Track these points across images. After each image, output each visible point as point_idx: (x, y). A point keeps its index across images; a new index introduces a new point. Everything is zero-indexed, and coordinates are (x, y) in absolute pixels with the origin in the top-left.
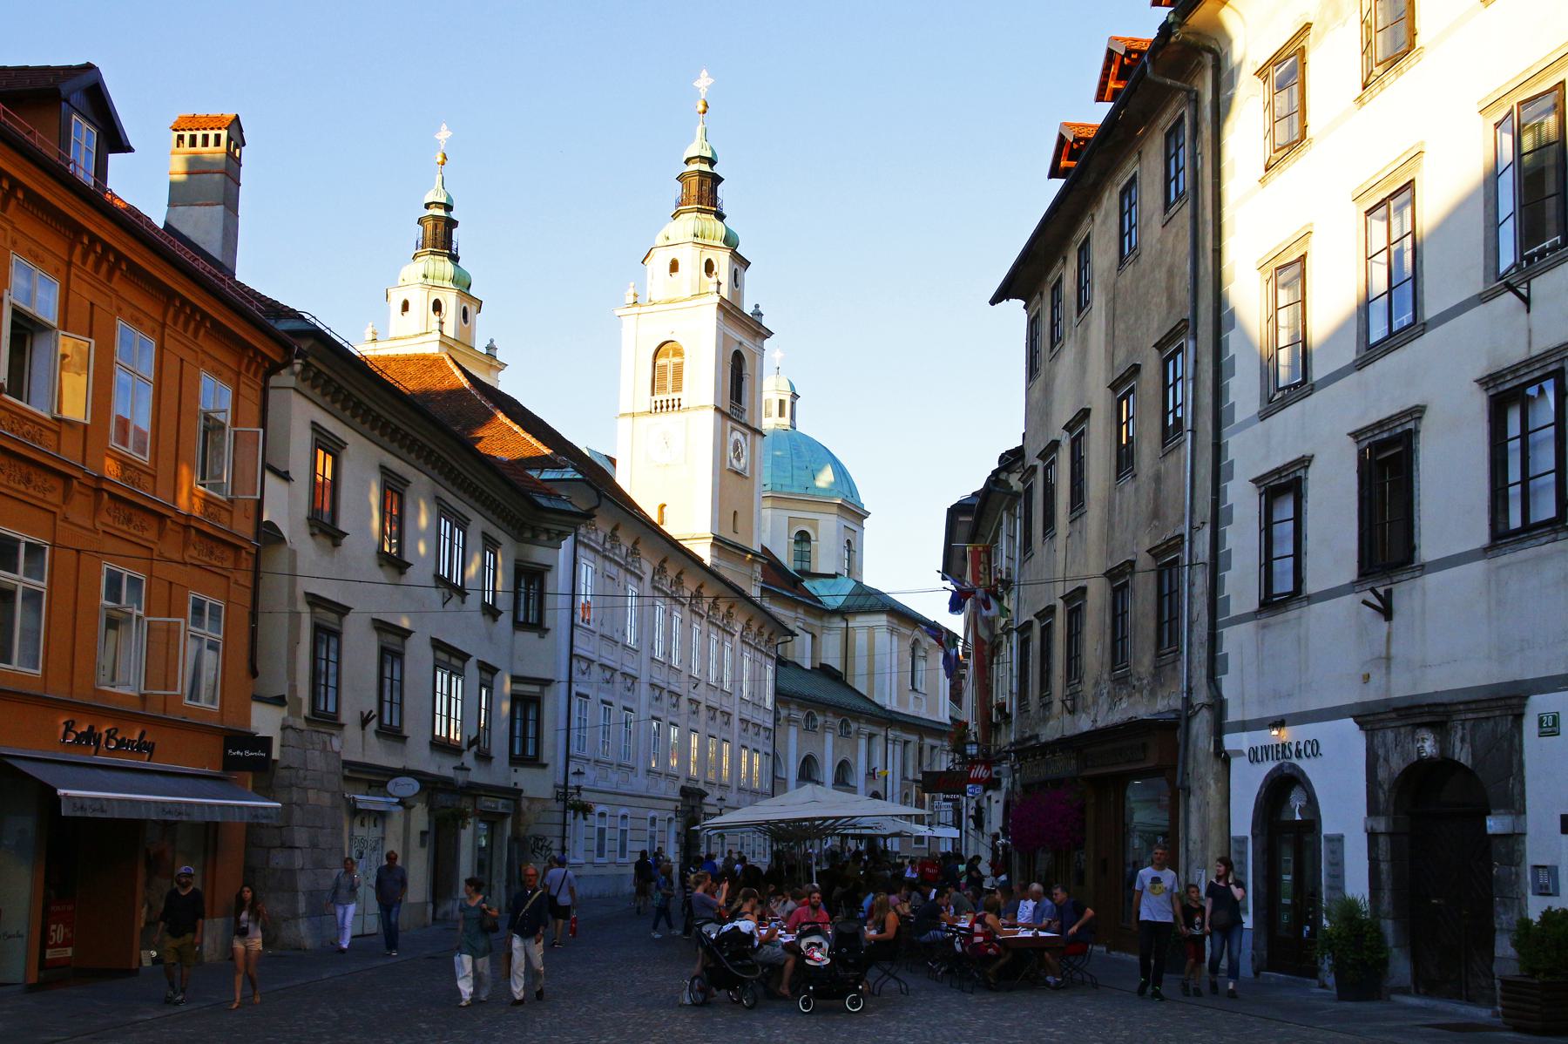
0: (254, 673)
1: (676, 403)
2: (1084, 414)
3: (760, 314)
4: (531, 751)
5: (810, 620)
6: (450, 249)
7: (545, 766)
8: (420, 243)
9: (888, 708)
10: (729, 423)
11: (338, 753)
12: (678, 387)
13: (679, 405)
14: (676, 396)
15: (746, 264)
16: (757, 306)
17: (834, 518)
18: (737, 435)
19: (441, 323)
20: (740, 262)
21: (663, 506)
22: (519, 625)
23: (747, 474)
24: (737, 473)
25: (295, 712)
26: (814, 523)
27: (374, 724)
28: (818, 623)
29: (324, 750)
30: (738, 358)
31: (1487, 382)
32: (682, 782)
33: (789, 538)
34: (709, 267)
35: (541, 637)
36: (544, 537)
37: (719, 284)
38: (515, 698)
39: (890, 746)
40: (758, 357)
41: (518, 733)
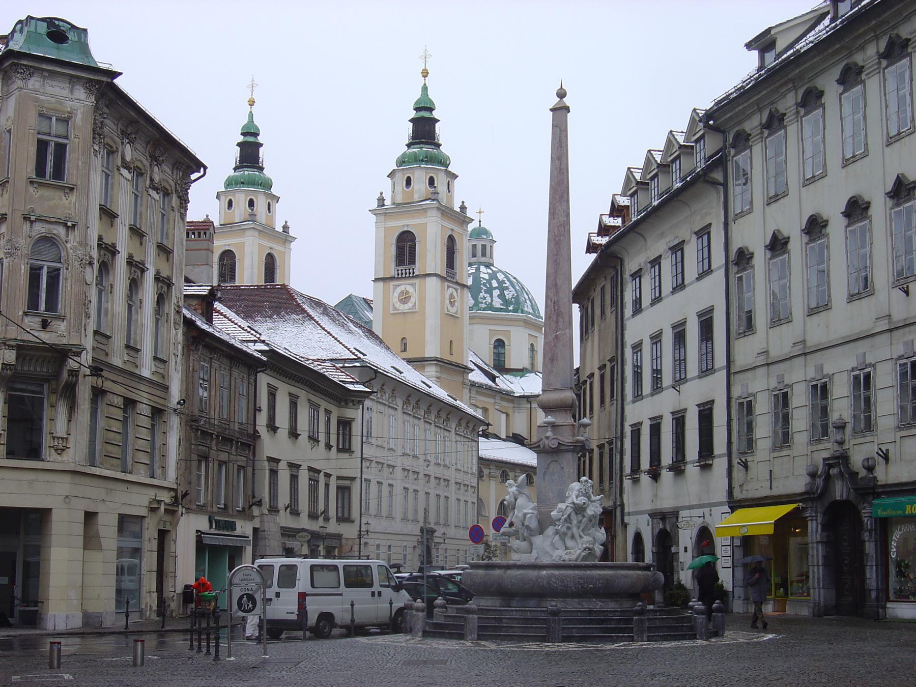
1: (411, 271)
2: (592, 375)
4: (346, 515)
5: (505, 404)
7: (353, 522)
8: (238, 159)
10: (446, 284)
11: (279, 523)
12: (413, 261)
13: (414, 273)
15: (455, 176)
16: (463, 202)
17: (521, 329)
22: (339, 450)
27: (288, 510)
28: (511, 405)
29: (275, 523)
30: (451, 239)
31: (673, 413)
32: (421, 524)
33: (490, 344)
34: (431, 181)
36: (351, 404)
38: (338, 488)
41: (340, 505)
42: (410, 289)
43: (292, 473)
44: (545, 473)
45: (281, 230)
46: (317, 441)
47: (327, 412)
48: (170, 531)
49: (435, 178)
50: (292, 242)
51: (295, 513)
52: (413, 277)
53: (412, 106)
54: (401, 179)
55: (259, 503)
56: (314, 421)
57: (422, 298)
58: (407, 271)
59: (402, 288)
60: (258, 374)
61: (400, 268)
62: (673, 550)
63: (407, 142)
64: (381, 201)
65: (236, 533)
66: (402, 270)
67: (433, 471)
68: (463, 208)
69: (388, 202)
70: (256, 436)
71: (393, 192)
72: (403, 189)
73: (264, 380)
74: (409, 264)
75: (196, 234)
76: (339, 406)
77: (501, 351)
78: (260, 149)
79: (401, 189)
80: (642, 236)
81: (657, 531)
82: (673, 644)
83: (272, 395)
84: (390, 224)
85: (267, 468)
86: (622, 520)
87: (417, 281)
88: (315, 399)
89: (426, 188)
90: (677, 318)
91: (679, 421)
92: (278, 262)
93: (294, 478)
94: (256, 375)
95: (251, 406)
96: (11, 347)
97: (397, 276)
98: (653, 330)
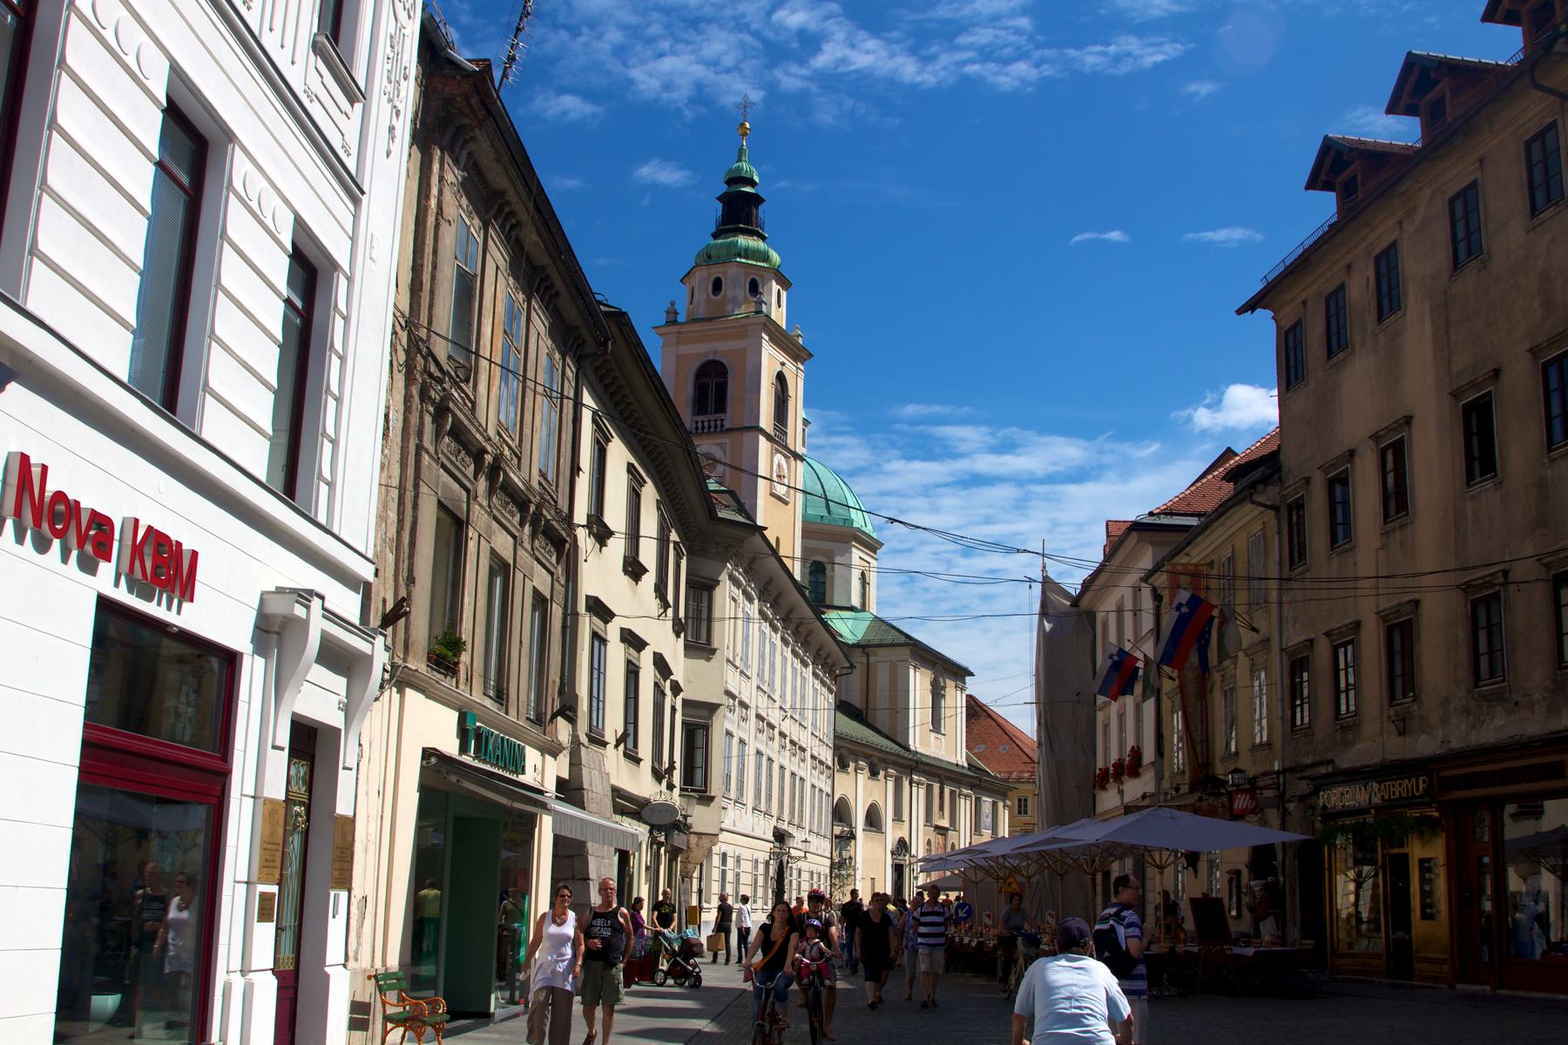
1: (719, 423)
9: (912, 748)
12: (721, 406)
13: (722, 426)
14: (722, 416)
18: (778, 458)
24: (779, 498)
26: (830, 555)
27: (622, 747)
30: (781, 378)
35: (709, 660)
39: (914, 789)
43: (630, 658)
52: (722, 431)
53: (723, 178)
54: (703, 277)
58: (712, 423)
61: (700, 418)
63: (713, 230)
64: (671, 312)
65: (522, 778)
66: (703, 422)
69: (681, 318)
71: (691, 303)
72: (708, 295)
74: (716, 412)
77: (820, 578)
87: (726, 440)
93: (632, 672)
97: (694, 431)
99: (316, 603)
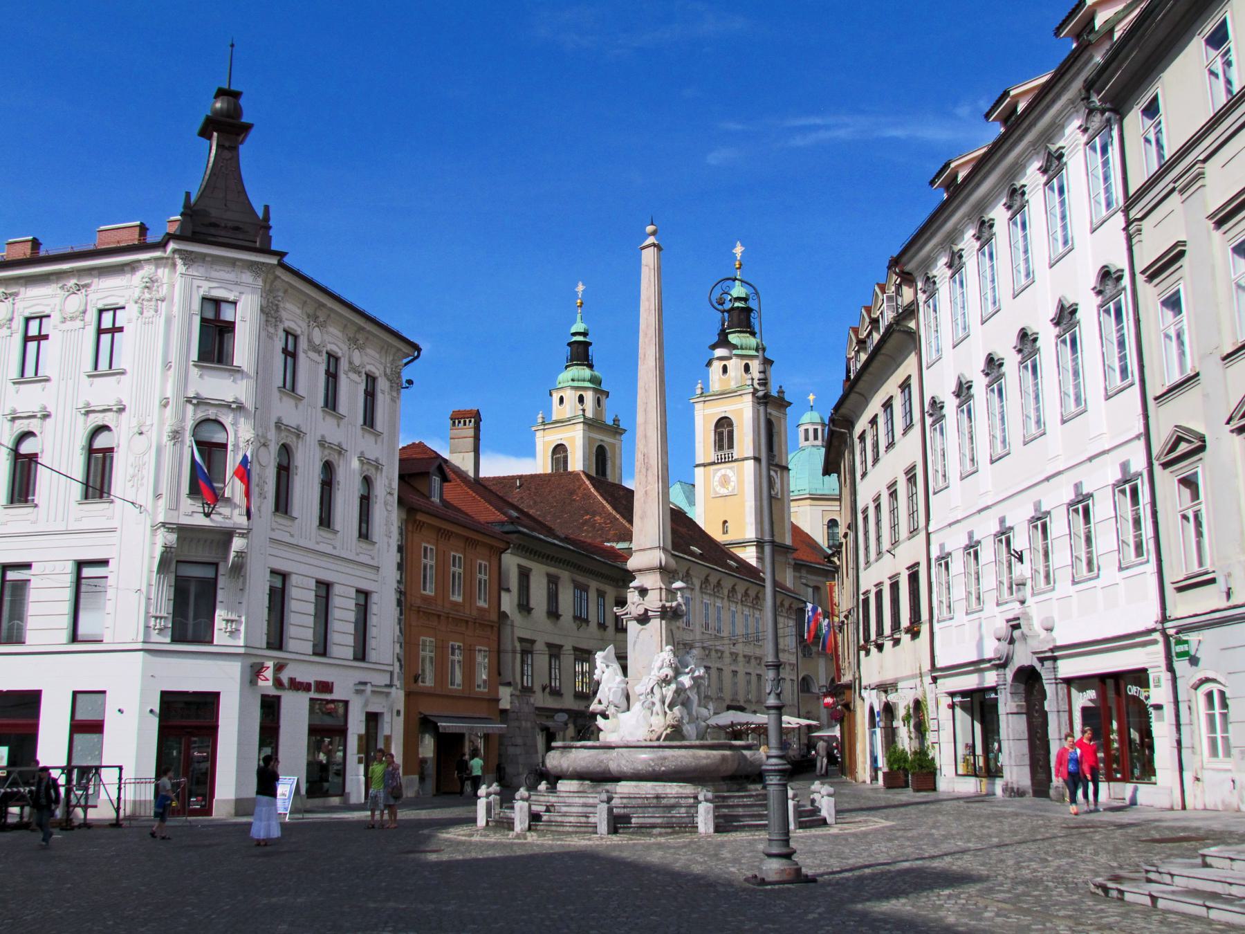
0: (499, 674)
3: (783, 392)
6: (588, 360)
11: (533, 704)
12: (731, 446)
14: (731, 451)
16: (781, 387)
19: (584, 410)
20: (767, 362)
21: (725, 522)
23: (779, 497)
25: (515, 689)
27: (548, 690)
29: (527, 703)
31: (890, 578)
37: (753, 379)
40: (782, 420)
42: (730, 473)
44: (634, 645)
45: (611, 423)
46: (587, 621)
47: (601, 594)
48: (382, 714)
49: (750, 365)
50: (622, 434)
51: (556, 693)
52: (732, 461)
55: (509, 684)
56: (580, 602)
57: (740, 482)
59: (723, 472)
60: (503, 555)
62: (895, 724)
67: (740, 648)
68: (781, 392)
70: (503, 616)
73: (511, 562)
75: (462, 421)
76: (617, 586)
78: (590, 349)
79: (718, 377)
80: (863, 395)
81: (882, 704)
82: (489, 852)
83: (524, 575)
84: (707, 412)
85: (518, 647)
86: (860, 693)
88: (581, 579)
89: (741, 375)
90: (889, 480)
91: (895, 587)
92: (609, 455)
94: (500, 556)
95: (496, 587)
96: (171, 530)
98: (873, 494)
99: (369, 685)
